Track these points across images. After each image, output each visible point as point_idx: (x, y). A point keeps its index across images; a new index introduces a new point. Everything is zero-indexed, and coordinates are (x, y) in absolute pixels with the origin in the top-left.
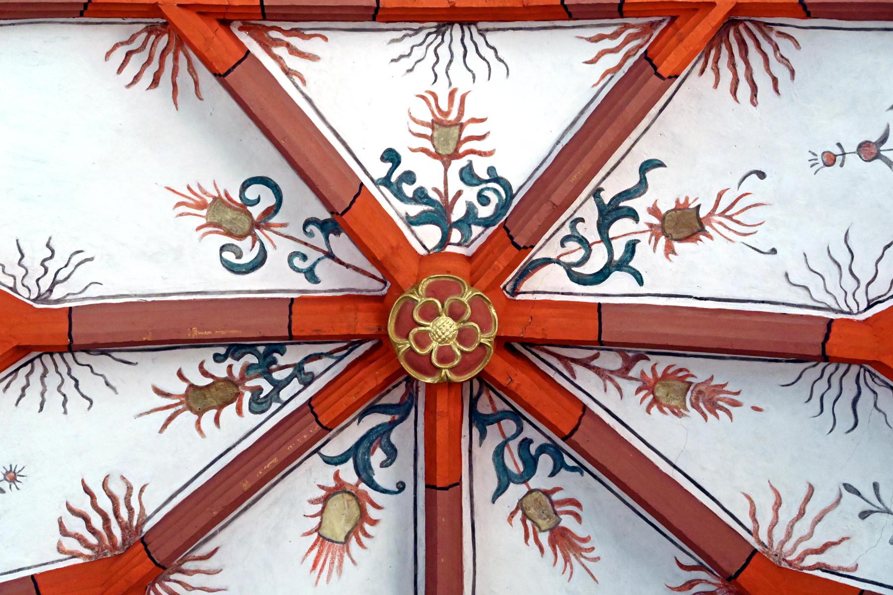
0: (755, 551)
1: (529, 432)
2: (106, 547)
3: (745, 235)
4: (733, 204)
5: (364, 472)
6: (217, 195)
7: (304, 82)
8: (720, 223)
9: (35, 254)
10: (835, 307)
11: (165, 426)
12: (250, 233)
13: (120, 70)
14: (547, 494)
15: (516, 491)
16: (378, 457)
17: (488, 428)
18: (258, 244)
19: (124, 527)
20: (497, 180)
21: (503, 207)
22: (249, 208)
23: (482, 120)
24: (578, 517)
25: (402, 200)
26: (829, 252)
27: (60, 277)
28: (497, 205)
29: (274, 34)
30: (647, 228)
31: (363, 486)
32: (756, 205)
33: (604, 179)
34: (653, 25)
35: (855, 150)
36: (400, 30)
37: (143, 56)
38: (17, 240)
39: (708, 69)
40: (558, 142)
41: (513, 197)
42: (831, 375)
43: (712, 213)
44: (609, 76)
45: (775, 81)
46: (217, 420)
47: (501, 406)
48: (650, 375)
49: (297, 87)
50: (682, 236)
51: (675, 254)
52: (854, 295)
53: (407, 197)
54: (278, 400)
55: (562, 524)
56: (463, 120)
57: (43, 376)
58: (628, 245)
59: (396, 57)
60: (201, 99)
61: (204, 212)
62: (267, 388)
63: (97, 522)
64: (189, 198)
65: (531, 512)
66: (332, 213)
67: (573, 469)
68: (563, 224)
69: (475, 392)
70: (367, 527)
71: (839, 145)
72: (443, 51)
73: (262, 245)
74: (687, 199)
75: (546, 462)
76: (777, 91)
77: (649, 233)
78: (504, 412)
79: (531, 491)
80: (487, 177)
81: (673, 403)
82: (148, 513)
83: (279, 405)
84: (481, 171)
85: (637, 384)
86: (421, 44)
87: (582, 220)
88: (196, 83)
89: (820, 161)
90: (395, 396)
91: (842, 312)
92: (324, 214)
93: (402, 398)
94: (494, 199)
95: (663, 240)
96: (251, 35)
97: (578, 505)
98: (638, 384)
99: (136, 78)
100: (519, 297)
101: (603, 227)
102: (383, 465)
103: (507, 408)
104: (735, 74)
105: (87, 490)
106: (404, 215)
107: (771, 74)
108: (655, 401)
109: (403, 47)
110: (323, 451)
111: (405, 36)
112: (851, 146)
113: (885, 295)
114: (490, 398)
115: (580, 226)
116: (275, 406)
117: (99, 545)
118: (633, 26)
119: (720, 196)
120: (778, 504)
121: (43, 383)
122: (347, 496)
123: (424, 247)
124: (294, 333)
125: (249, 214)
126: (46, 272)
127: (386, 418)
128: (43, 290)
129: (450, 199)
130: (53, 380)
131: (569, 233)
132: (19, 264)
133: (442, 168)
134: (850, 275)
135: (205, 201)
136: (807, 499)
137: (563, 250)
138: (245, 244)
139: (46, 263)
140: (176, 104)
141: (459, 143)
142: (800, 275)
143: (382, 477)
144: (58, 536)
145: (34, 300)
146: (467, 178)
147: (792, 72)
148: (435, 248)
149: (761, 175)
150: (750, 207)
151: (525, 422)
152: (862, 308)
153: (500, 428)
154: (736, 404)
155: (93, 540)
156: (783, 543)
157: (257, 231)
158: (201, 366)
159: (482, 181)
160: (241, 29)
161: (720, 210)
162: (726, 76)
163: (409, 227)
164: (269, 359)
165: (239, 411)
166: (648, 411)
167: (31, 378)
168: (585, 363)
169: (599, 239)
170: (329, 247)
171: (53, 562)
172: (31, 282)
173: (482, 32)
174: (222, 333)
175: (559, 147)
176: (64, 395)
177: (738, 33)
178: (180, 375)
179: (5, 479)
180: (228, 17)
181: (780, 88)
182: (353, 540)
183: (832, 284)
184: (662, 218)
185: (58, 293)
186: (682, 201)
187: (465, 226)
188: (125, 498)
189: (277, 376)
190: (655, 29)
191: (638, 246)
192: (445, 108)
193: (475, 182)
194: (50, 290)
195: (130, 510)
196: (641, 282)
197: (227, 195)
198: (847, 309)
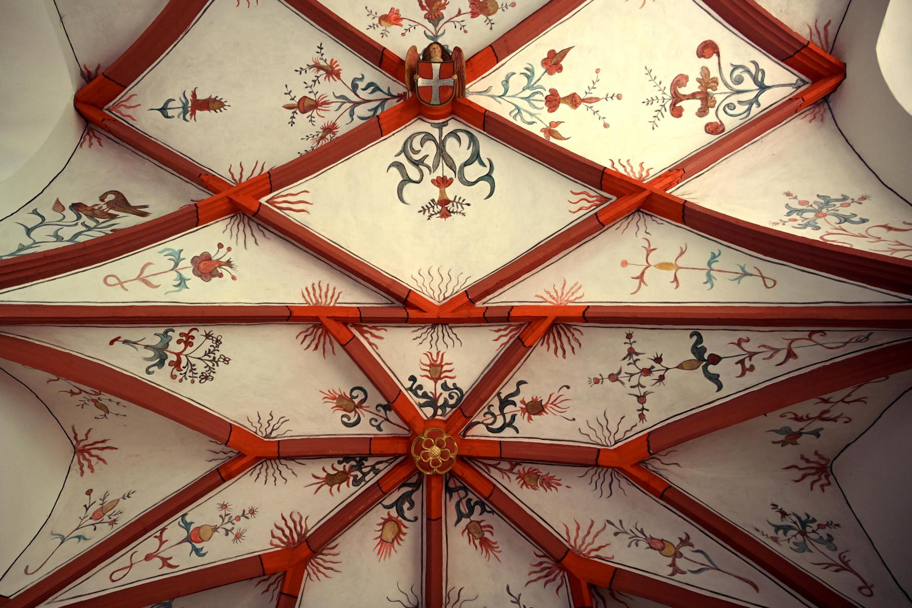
0: (569, 549)
1: (470, 496)
2: (291, 543)
3: (561, 412)
4: (556, 399)
5: (400, 512)
6: (340, 394)
7: (377, 348)
8: (551, 407)
9: (265, 418)
10: (601, 443)
11: (317, 491)
12: (354, 410)
13: (302, 343)
14: (479, 522)
15: (465, 522)
16: (406, 505)
17: (453, 494)
18: (357, 415)
19: (298, 534)
20: (457, 388)
21: (459, 400)
22: (354, 400)
23: (451, 364)
24: (492, 533)
25: (417, 397)
26: (597, 420)
27: (275, 428)
28: (457, 399)
29: (365, 329)
30: (520, 409)
31: (400, 518)
32: (566, 400)
33: (501, 388)
34: (521, 325)
36: (417, 327)
37: (311, 337)
38: (258, 413)
40: (482, 373)
41: (464, 395)
42: (600, 472)
43: (547, 403)
44: (503, 346)
45: (573, 348)
46: (338, 489)
47: (459, 484)
48: (522, 472)
49: (374, 350)
50: (535, 413)
51: (532, 420)
52: (609, 438)
53: (418, 395)
54: (364, 480)
55: (485, 536)
56: (443, 364)
57: (267, 469)
58: (512, 416)
59: (415, 338)
60: (335, 355)
61: (335, 401)
62: (360, 475)
63: (287, 532)
64: (329, 395)
65: (472, 530)
66: (388, 402)
67: (489, 512)
68: (485, 407)
69: (448, 479)
70: (401, 536)
71: (600, 375)
72: (435, 335)
73: (359, 415)
74: (537, 397)
75: (478, 509)
76: (574, 353)
77: (521, 412)
78: (460, 487)
79: (471, 521)
80: (453, 387)
81: (532, 484)
82: (309, 528)
83: (365, 483)
84: (450, 385)
85: (516, 476)
86: (425, 333)
87: (493, 406)
88: (333, 348)
89: (593, 381)
90: (414, 480)
91: (604, 446)
92: (385, 403)
93: (417, 481)
94: (456, 397)
95: (527, 414)
96: (356, 329)
97: (492, 528)
98: (517, 476)
99: (308, 346)
100: (466, 438)
101: (501, 409)
102: (409, 509)
103: (461, 485)
104: (556, 346)
105: (283, 518)
106: (418, 403)
107: (571, 345)
108: (525, 483)
109: (418, 334)
110: (383, 503)
111: (419, 329)
112: (606, 375)
114: (454, 481)
115: (491, 408)
116: (363, 483)
117: (287, 542)
118: (513, 326)
119: (551, 396)
120: (578, 529)
121: (266, 472)
122: (393, 522)
123: (426, 416)
124: (372, 452)
125: (354, 402)
126: (269, 426)
127: (409, 489)
128: (268, 433)
129: (437, 396)
130: (271, 471)
131: (487, 411)
132: (259, 422)
133: (434, 383)
134: (607, 430)
135: (335, 396)
136: (591, 527)
137: (485, 418)
138: (352, 415)
139: (269, 422)
140: (324, 356)
141: (441, 373)
142: (585, 430)
143: (408, 514)
144: (271, 538)
145: (264, 437)
146: (444, 388)
147: (580, 345)
148: (431, 417)
149: (568, 387)
151: (469, 492)
153: (458, 494)
154: (559, 485)
155: (285, 540)
156: (581, 546)
157: (357, 409)
158: (333, 464)
159: (451, 389)
160: (351, 326)
161: (551, 402)
162: (552, 346)
163: (420, 408)
164: (360, 463)
165: (348, 485)
166: (521, 487)
167: (262, 470)
168: (495, 467)
169: (500, 414)
170: (387, 416)
171: (268, 549)
172: (263, 430)
173: (450, 328)
174: (341, 452)
175: (483, 375)
176: (275, 477)
177: (557, 328)
178: (324, 469)
179: (249, 513)
180: (347, 322)
181: (575, 351)
182: (395, 542)
183: (599, 434)
184: (526, 405)
185: (273, 435)
186: (534, 398)
187: (443, 408)
188: (299, 522)
189: (364, 470)
191: (516, 417)
192: (435, 358)
193: (448, 389)
194: (271, 433)
195: (301, 527)
196: (518, 432)
197: (344, 394)
198: (606, 444)
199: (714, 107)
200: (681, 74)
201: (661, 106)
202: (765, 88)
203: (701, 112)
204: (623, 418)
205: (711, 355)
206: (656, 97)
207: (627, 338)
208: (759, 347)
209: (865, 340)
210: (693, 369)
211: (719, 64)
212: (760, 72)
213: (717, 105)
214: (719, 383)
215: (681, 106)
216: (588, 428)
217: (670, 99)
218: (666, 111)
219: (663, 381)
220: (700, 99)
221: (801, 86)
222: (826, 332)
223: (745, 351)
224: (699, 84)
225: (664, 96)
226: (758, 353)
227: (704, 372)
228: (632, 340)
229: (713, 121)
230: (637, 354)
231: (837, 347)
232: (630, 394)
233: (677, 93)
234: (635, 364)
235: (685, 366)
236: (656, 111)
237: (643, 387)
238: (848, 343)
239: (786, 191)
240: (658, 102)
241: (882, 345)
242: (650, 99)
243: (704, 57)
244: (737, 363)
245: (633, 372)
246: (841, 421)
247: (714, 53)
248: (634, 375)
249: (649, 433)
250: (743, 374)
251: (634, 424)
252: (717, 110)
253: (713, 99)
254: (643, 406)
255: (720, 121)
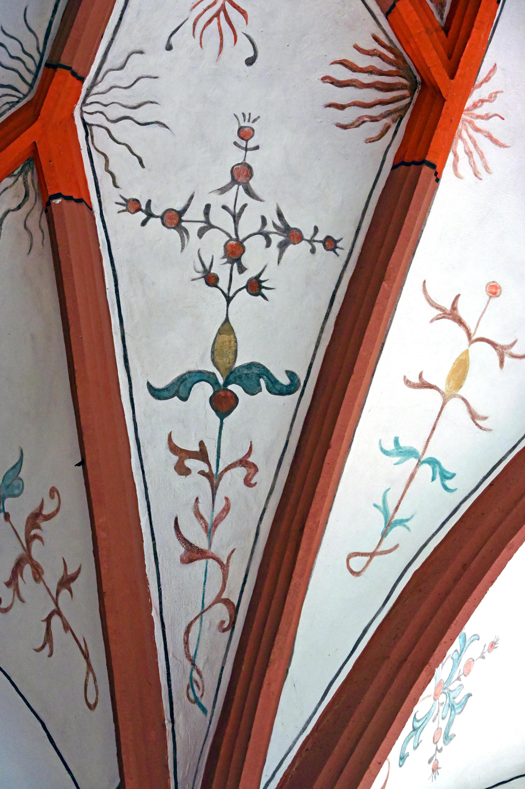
3: (195, 24)
26: (151, 102)
35: (248, 161)
39: (376, 46)
42: (24, 63)
45: (342, 107)
52: (101, 113)
71: (257, 148)
76: (330, 105)
89: (246, 124)
107: (349, 105)
113: (93, 143)
119: (243, 13)
134: (122, 115)
150: (222, 39)
152: (85, 116)
161: (228, 6)
162: (363, 61)
177: (403, 87)
190: (436, 7)
198: (88, 101)
204: (141, 162)
205: (236, 400)
207: (328, 238)
208: (227, 499)
209: (192, 697)
210: (213, 353)
214: (166, 394)
216: (139, 75)
219: (203, 280)
222: (228, 633)
223: (226, 470)
226: (214, 494)
227: (200, 372)
228: (319, 247)
230: (283, 246)
231: (186, 643)
232: (192, 197)
234: (260, 233)
235: (225, 337)
237: (201, 233)
238: (193, 664)
239: (499, 645)
241: (173, 722)
244: (201, 444)
245: (241, 221)
246: (7, 595)
248: (236, 221)
249: (91, 209)
250: (174, 449)
251: (119, 183)
254: (158, 217)
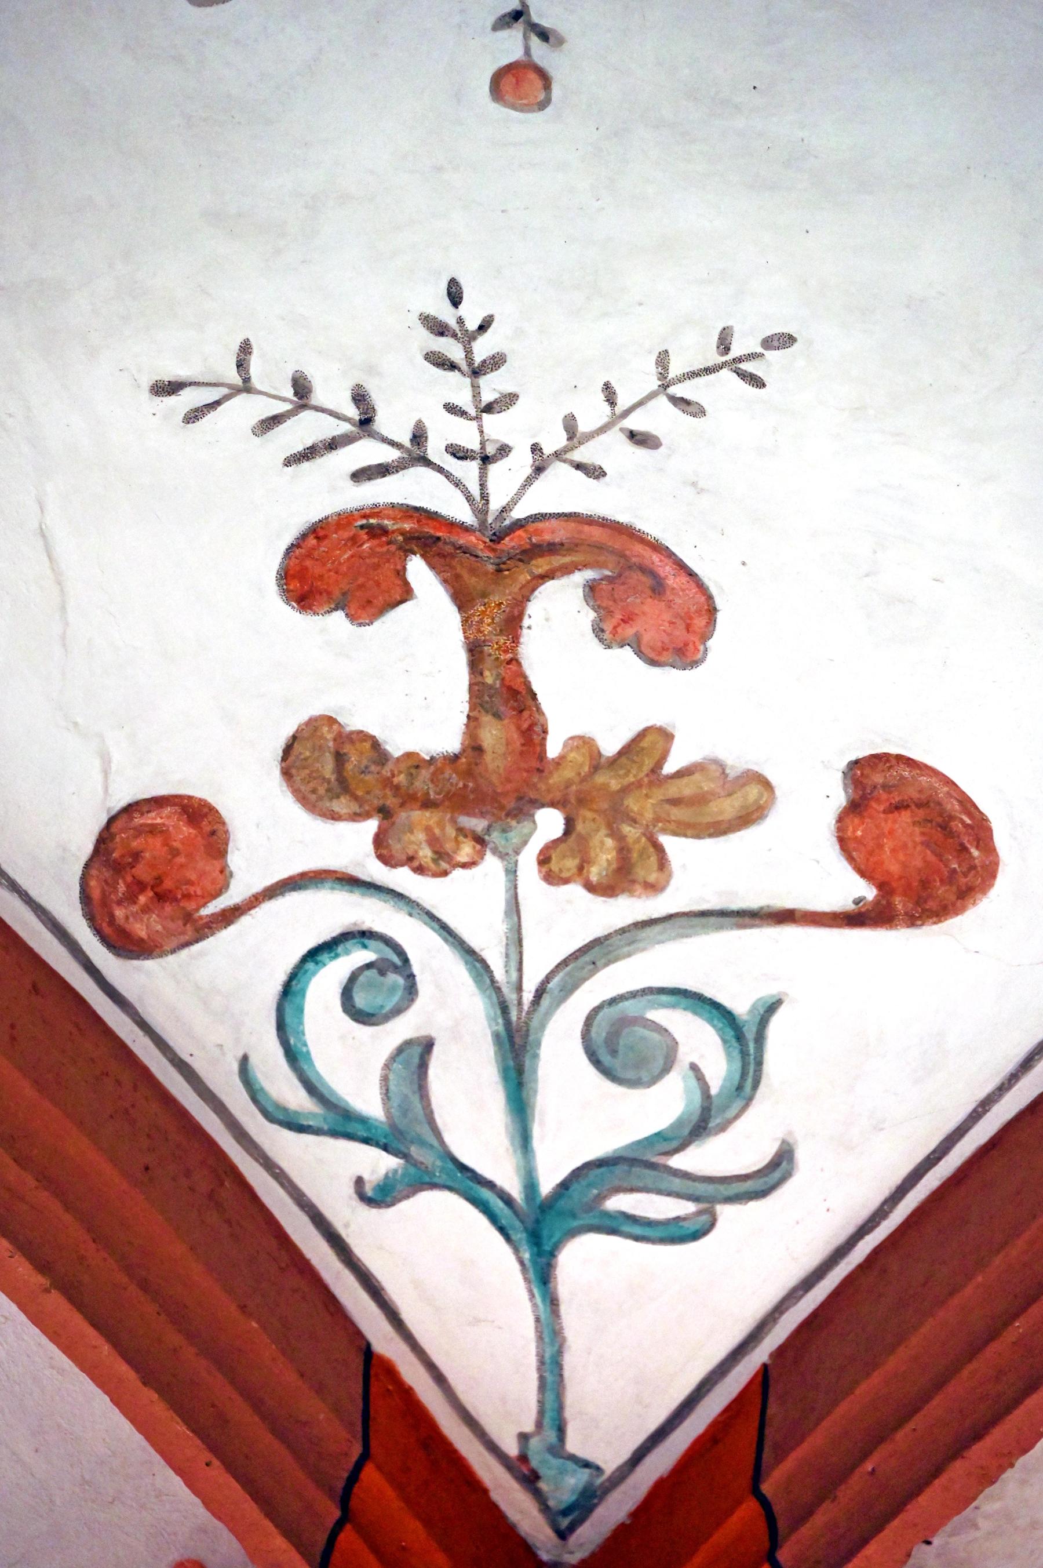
199: (386, 858)
200: (712, 611)
201: (419, 437)
202: (535, 1238)
203: (340, 758)
206: (509, 400)
211: (785, 917)
212: (686, 1208)
213: (402, 879)
215: (406, 593)
217: (480, 504)
218: (361, 475)
220: (473, 747)
221: (538, 1495)
224: (610, 746)
225: (520, 462)
229: (235, 860)
233: (541, 565)
236: (360, 398)
240: (452, 409)
242: (483, 348)
243: (854, 808)
247: (884, 887)
252: (351, 882)
253: (466, 852)
255: (230, 916)
